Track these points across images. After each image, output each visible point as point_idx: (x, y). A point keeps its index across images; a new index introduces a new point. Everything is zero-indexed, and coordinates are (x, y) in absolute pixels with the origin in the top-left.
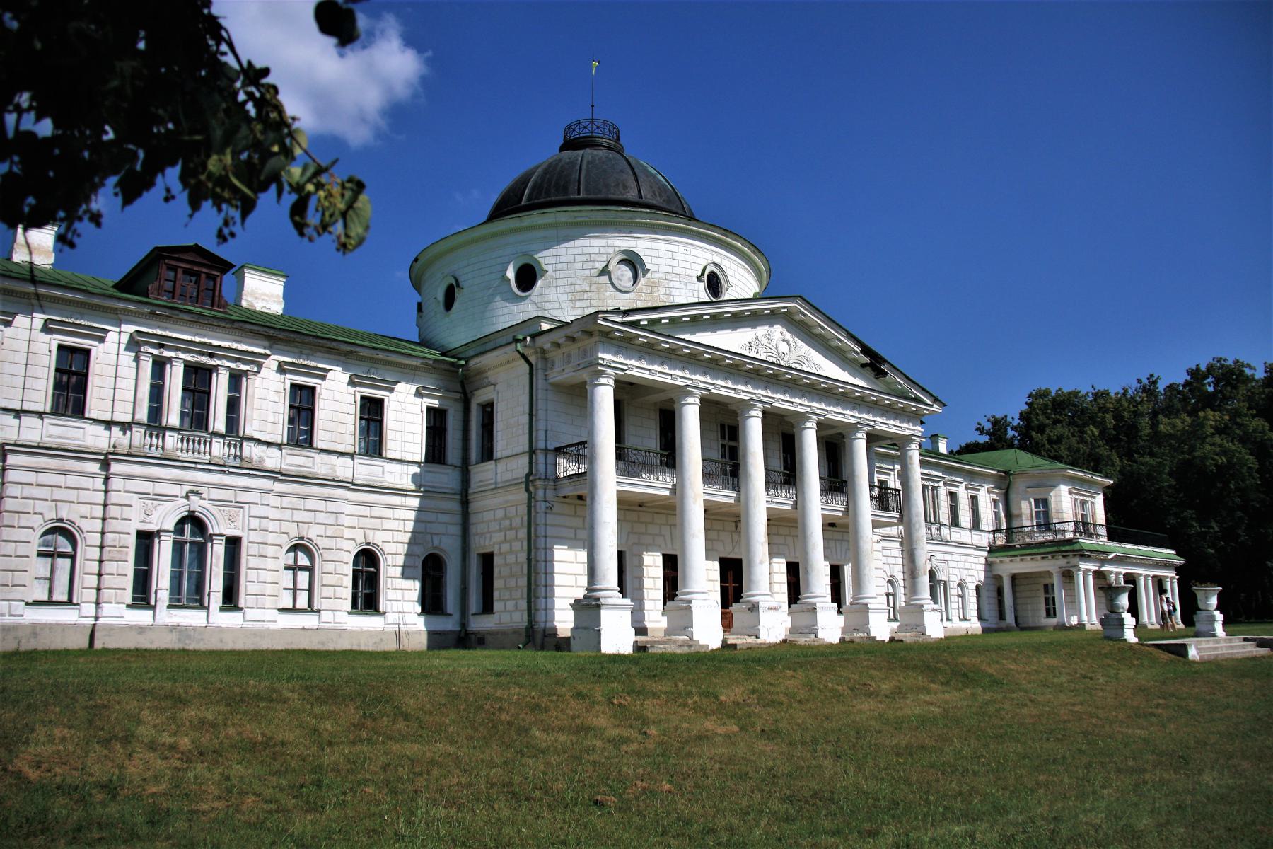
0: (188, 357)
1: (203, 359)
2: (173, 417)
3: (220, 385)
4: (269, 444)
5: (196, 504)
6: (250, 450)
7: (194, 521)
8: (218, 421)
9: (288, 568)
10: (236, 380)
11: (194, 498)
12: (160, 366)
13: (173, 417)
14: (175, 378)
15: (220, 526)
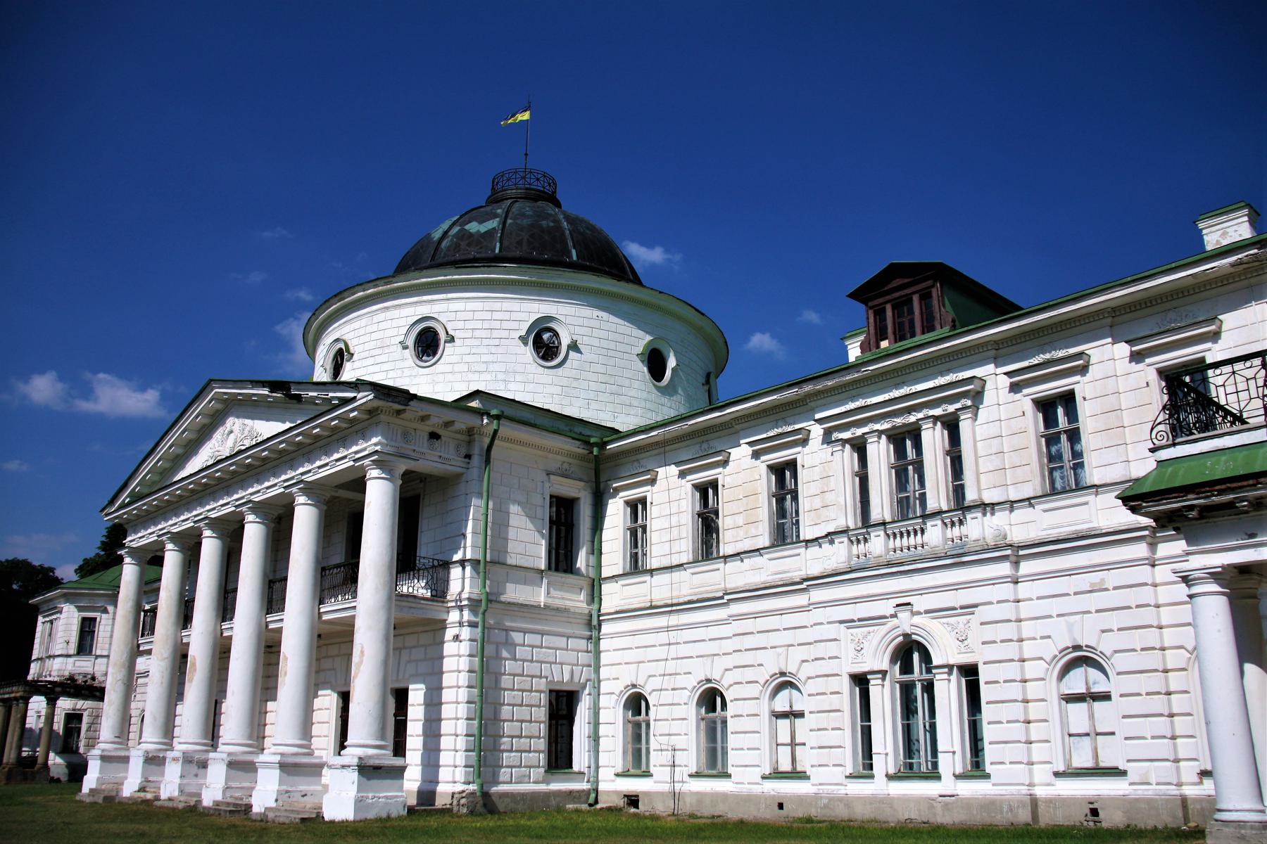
0: (885, 425)
1: (899, 421)
2: (881, 506)
3: (933, 440)
4: (1012, 505)
5: (905, 623)
6: (977, 528)
7: (909, 652)
8: (938, 497)
9: (800, 715)
10: (951, 426)
11: (904, 615)
12: (860, 447)
13: (881, 506)
14: (880, 453)
15: (946, 648)
